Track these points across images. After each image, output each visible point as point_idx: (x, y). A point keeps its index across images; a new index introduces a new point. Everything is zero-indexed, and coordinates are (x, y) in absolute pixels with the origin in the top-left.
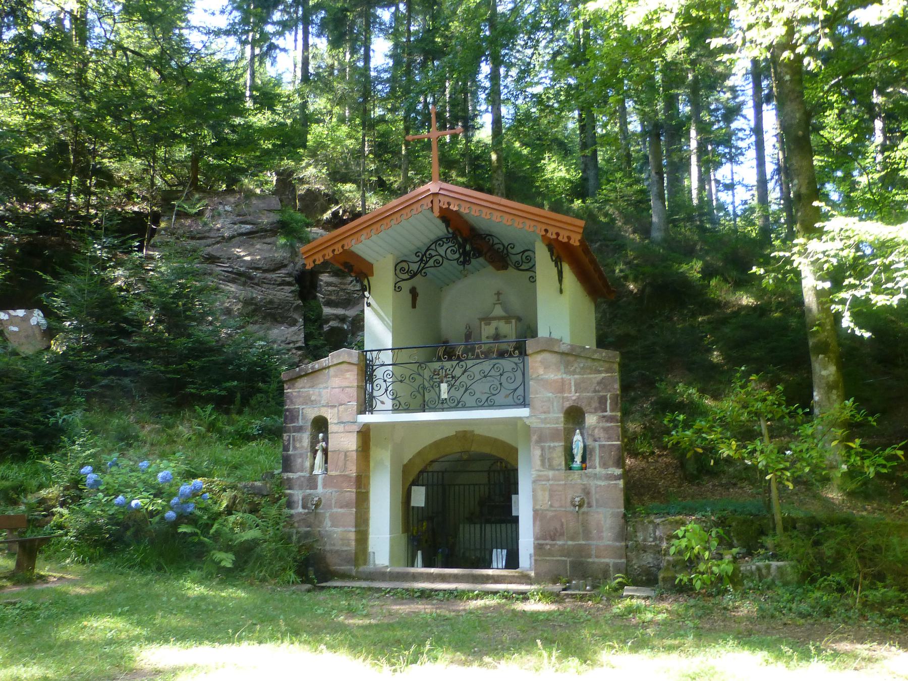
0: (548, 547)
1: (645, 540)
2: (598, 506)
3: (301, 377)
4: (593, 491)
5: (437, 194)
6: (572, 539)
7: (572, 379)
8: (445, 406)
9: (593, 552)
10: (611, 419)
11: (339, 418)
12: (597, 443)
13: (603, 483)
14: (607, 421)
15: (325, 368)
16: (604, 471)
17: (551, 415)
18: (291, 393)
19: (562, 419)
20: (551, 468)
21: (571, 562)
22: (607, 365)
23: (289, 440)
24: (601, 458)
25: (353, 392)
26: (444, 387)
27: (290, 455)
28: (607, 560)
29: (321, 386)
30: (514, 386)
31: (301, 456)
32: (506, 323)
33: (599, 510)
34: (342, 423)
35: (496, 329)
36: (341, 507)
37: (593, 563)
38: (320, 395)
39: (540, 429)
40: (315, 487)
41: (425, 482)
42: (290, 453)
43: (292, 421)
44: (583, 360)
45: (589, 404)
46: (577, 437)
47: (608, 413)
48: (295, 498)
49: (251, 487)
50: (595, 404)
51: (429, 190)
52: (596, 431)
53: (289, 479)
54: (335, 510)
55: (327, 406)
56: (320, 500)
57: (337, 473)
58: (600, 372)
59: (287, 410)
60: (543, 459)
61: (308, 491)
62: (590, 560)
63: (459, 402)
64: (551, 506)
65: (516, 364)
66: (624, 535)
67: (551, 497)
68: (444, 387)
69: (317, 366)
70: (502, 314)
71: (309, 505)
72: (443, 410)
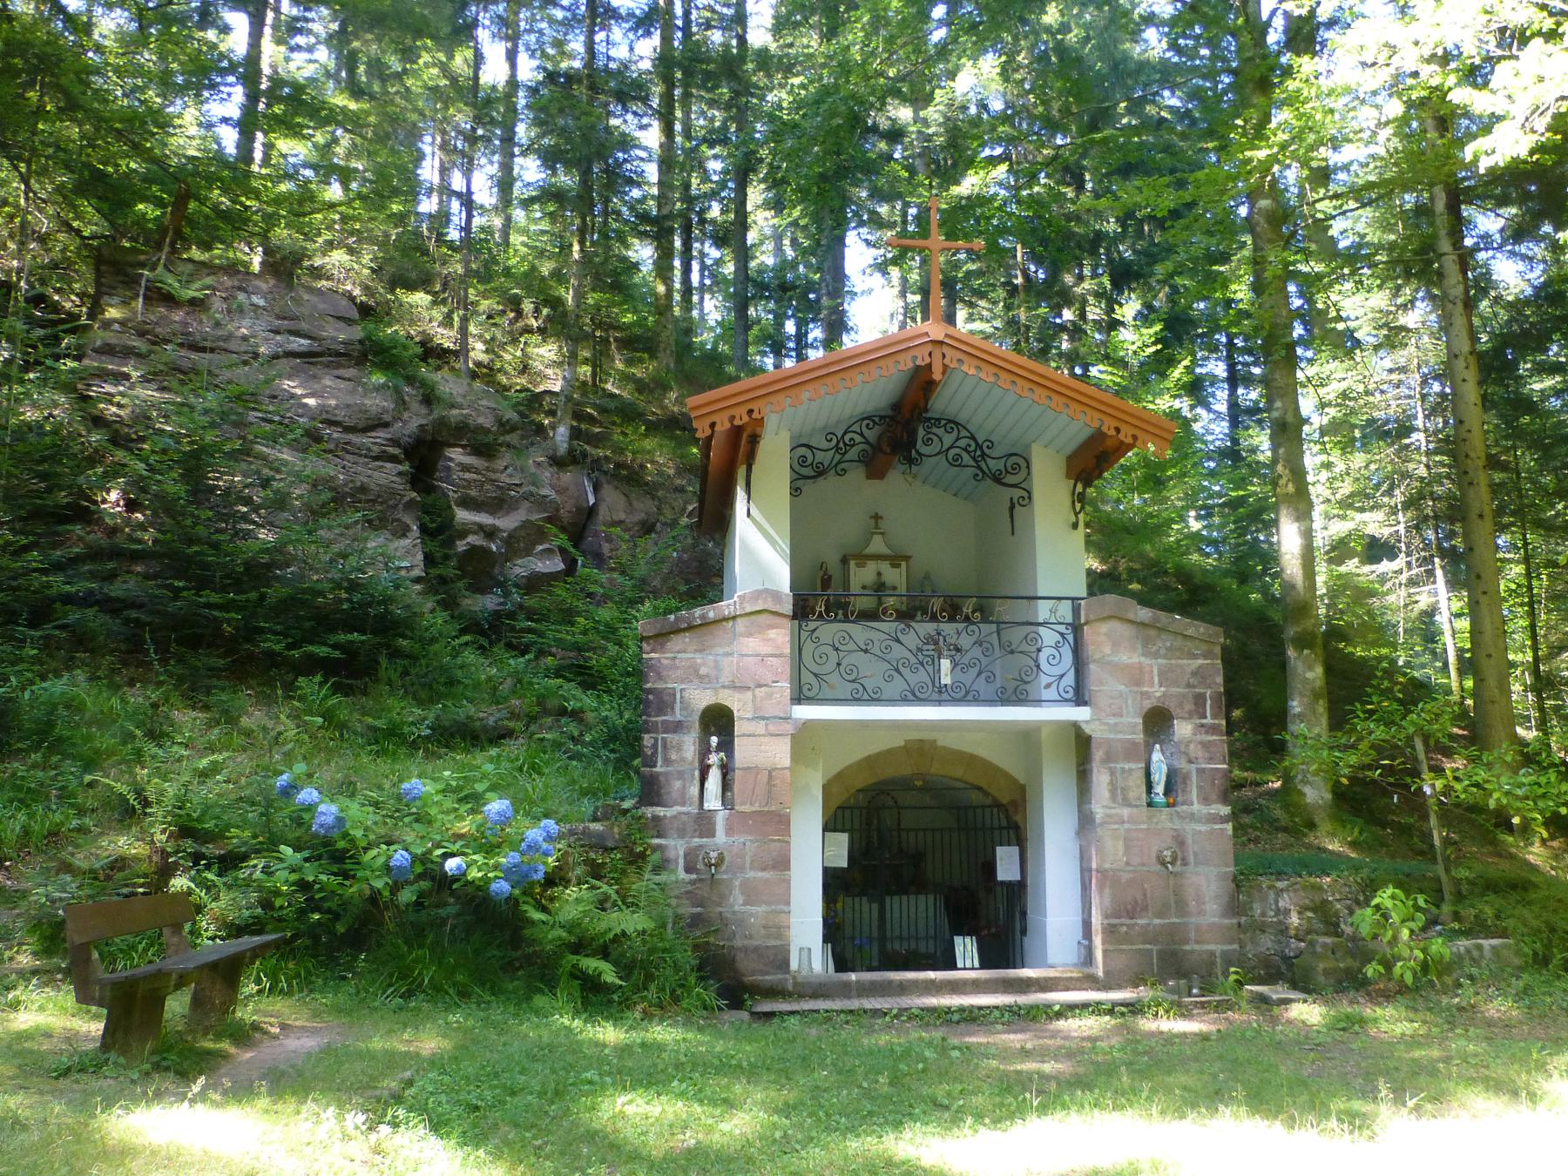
0: (1125, 929)
1: (1263, 914)
2: (1196, 864)
3: (679, 631)
4: (1190, 841)
5: (942, 343)
6: (1160, 915)
7: (1154, 666)
8: (945, 696)
9: (1192, 935)
10: (1213, 729)
11: (756, 709)
12: (1193, 766)
13: (1203, 828)
14: (1207, 733)
15: (726, 619)
16: (1205, 810)
17: (1125, 720)
18: (659, 660)
19: (1141, 727)
20: (1127, 803)
21: (1160, 953)
22: (1204, 647)
23: (655, 746)
24: (1200, 788)
25: (783, 667)
26: (946, 664)
27: (658, 774)
28: (1212, 947)
29: (720, 651)
30: (1057, 671)
31: (681, 775)
32: (894, 566)
33: (1200, 869)
34: (763, 718)
35: (879, 574)
36: (763, 869)
37: (1192, 952)
38: (717, 666)
39: (1108, 740)
40: (711, 833)
41: (848, 826)
42: (658, 769)
43: (661, 711)
44: (1171, 637)
45: (1181, 705)
46: (1157, 756)
47: (1208, 721)
48: (671, 854)
49: (583, 833)
50: (1189, 706)
51: (927, 334)
52: (1192, 746)
53: (656, 818)
54: (751, 874)
55: (734, 687)
56: (721, 858)
57: (756, 808)
58: (1195, 657)
59: (649, 691)
60: (1113, 791)
61: (697, 841)
62: (1188, 948)
63: (967, 693)
64: (1127, 864)
65: (1062, 635)
66: (1235, 907)
67: (1127, 848)
68: (946, 664)
69: (711, 615)
70: (885, 550)
71: (700, 866)
72: (940, 703)
